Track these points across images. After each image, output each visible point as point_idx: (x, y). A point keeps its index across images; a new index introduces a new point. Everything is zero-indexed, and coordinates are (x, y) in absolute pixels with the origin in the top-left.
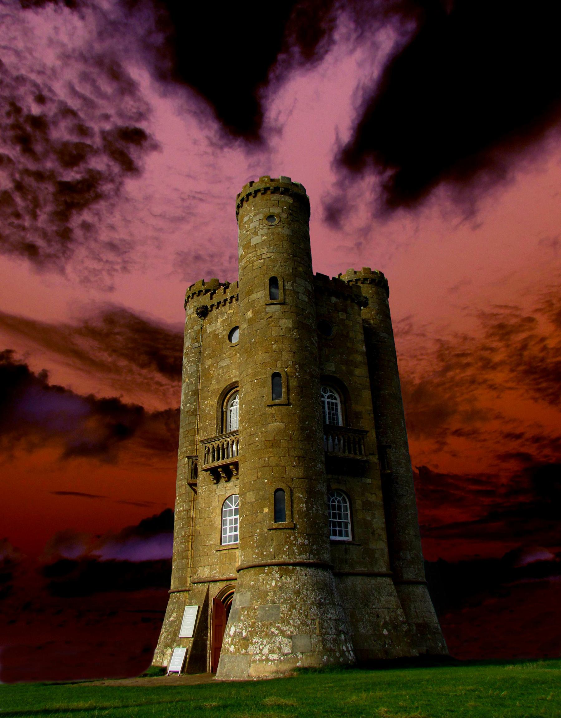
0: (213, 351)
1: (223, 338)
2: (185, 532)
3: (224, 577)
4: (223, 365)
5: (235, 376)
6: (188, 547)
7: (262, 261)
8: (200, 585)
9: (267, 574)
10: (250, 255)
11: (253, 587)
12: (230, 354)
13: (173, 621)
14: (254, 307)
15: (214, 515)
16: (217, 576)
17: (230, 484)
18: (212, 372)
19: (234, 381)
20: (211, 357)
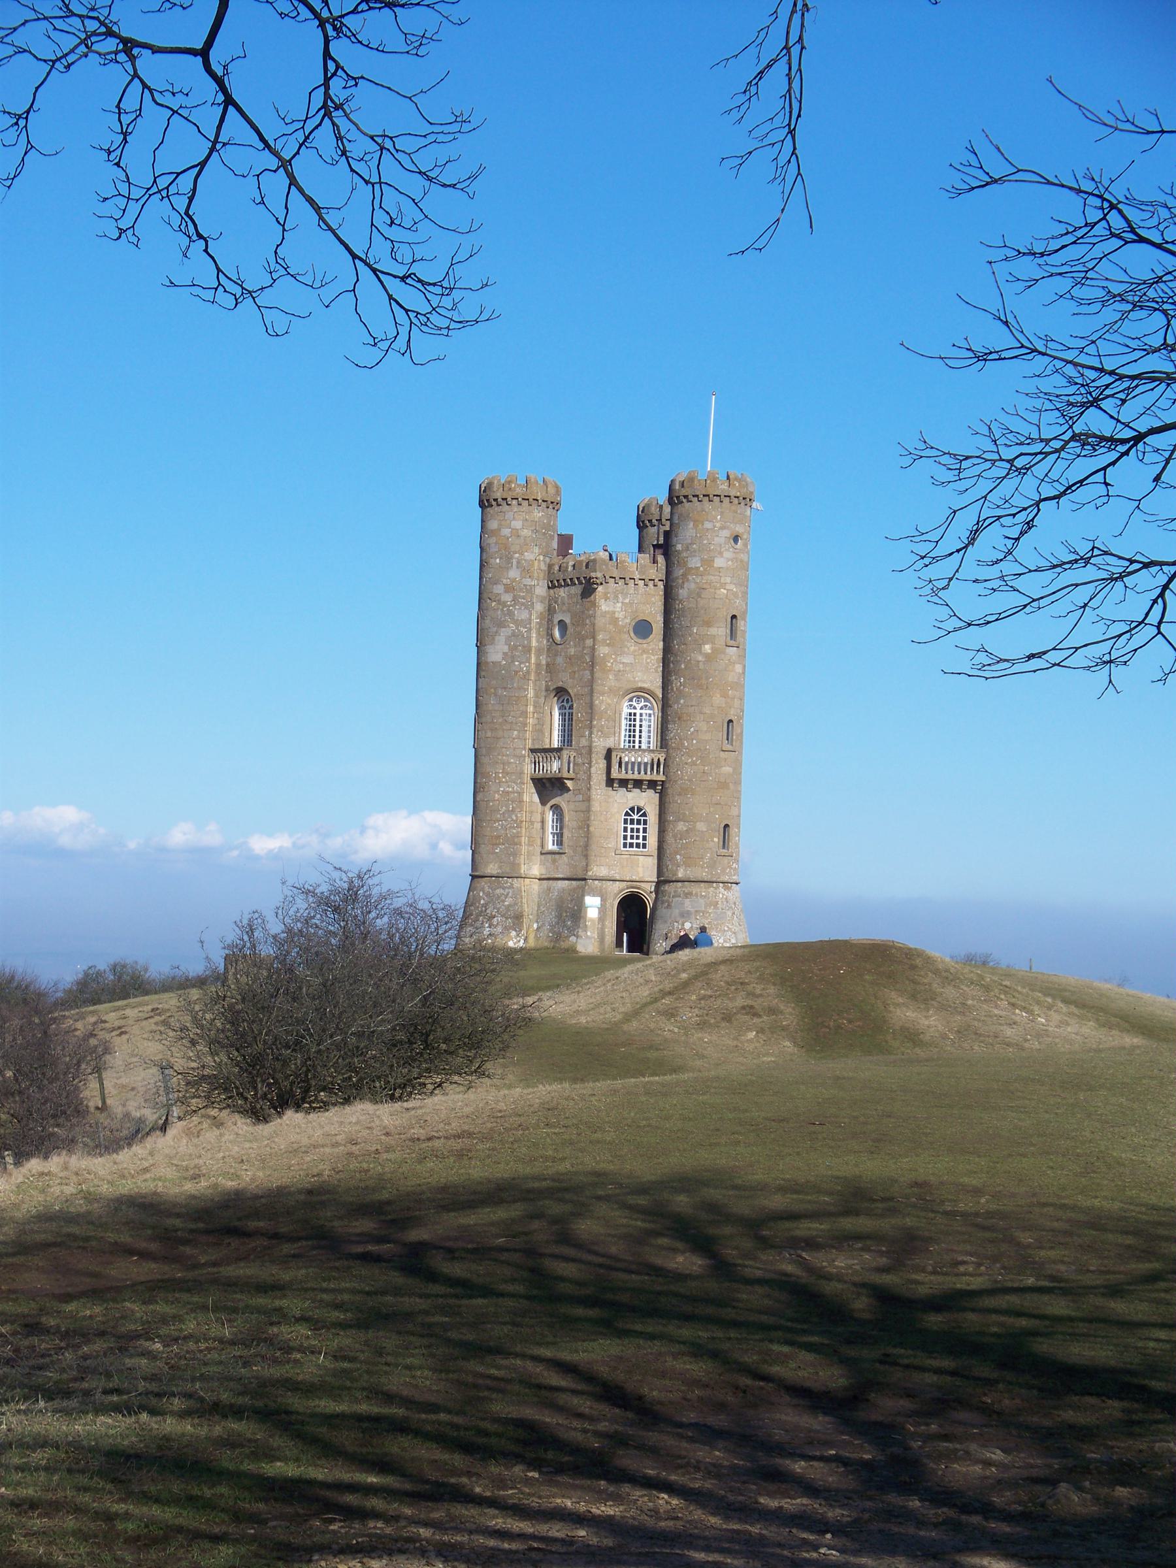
0: (610, 639)
1: (624, 627)
2: (516, 816)
3: (628, 879)
4: (625, 661)
5: (644, 682)
6: (521, 833)
7: (725, 592)
8: (596, 882)
9: (716, 889)
10: (712, 578)
11: (705, 896)
12: (635, 651)
13: (509, 906)
14: (713, 643)
15: (613, 820)
16: (618, 878)
17: (630, 795)
18: (609, 664)
19: (640, 685)
20: (608, 645)
